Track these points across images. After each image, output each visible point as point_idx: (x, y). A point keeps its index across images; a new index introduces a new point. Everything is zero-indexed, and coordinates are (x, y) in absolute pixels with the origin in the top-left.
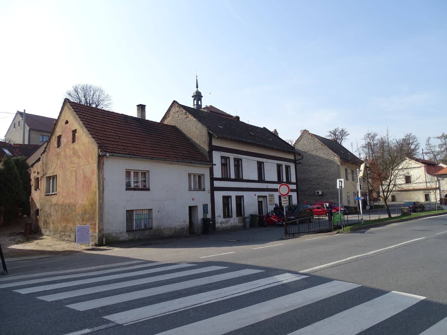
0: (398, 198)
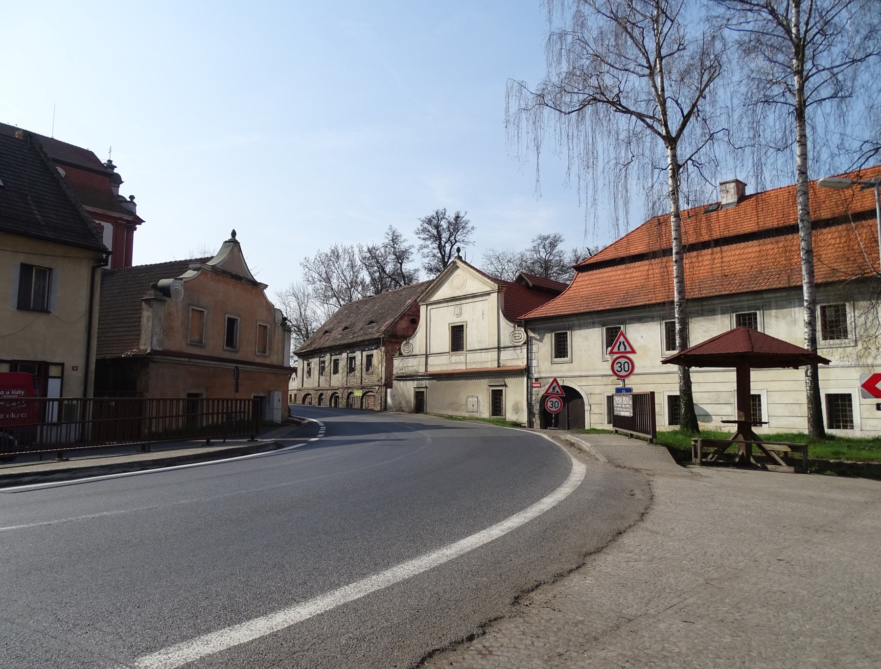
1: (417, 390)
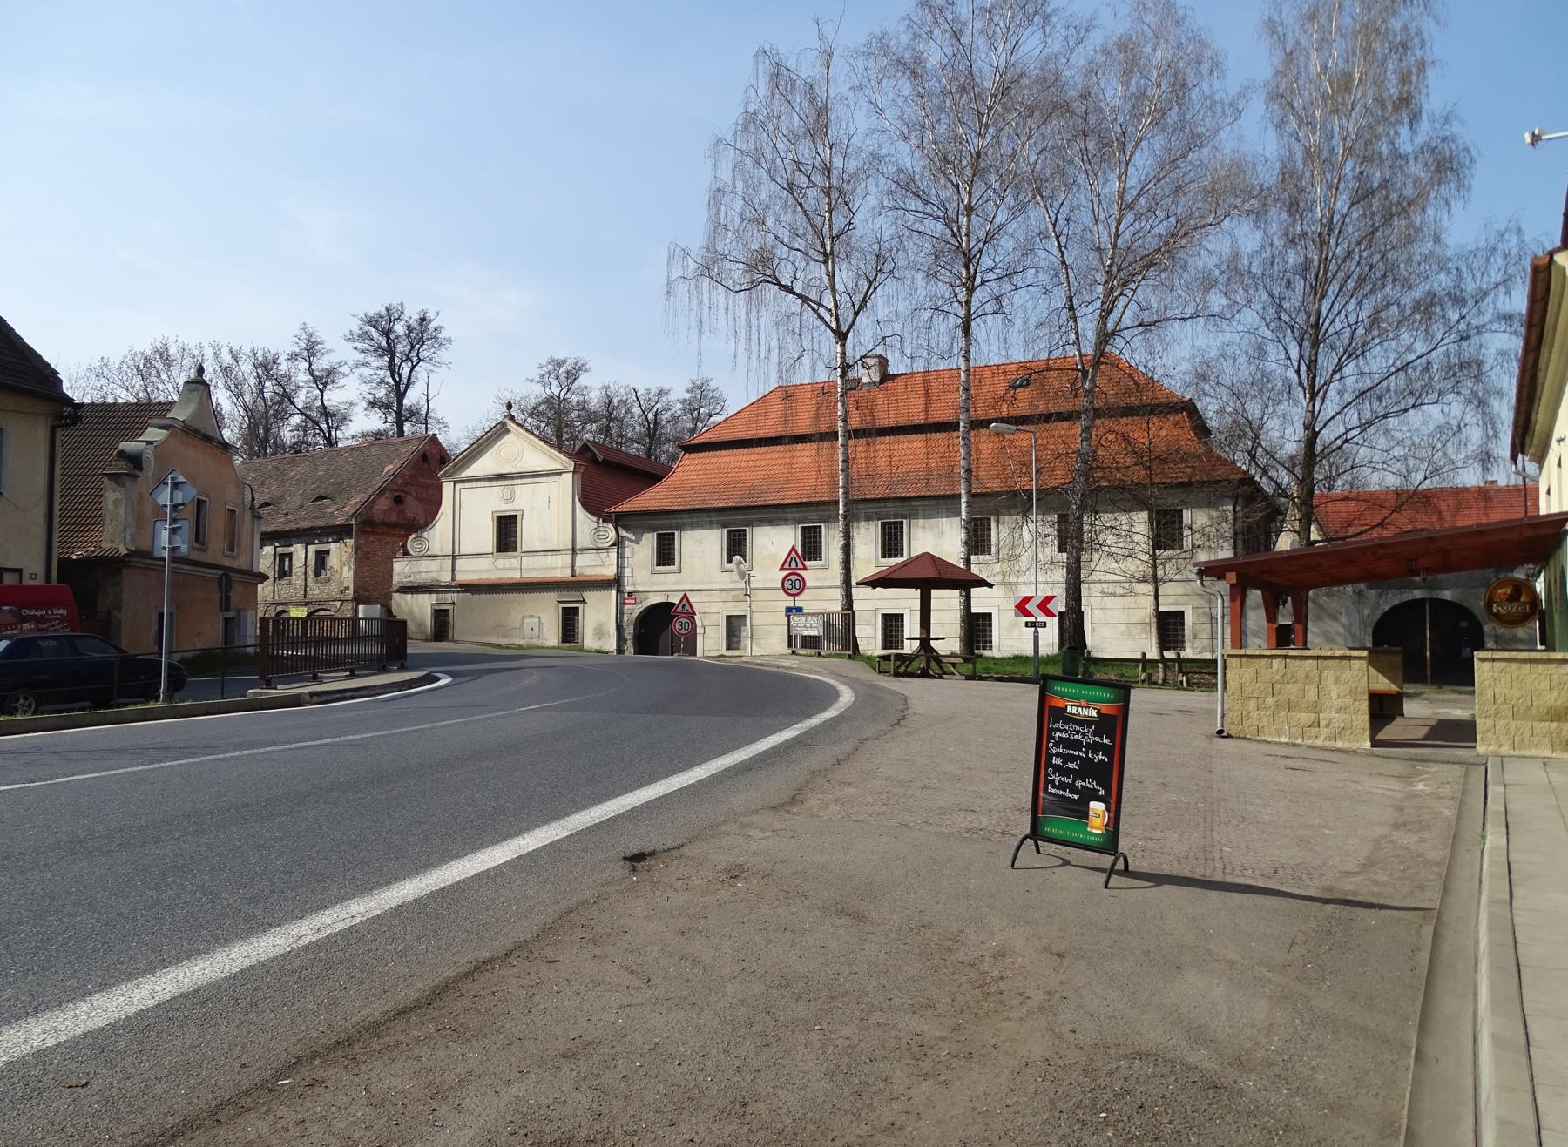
0: (460, 624)
1: (437, 607)
